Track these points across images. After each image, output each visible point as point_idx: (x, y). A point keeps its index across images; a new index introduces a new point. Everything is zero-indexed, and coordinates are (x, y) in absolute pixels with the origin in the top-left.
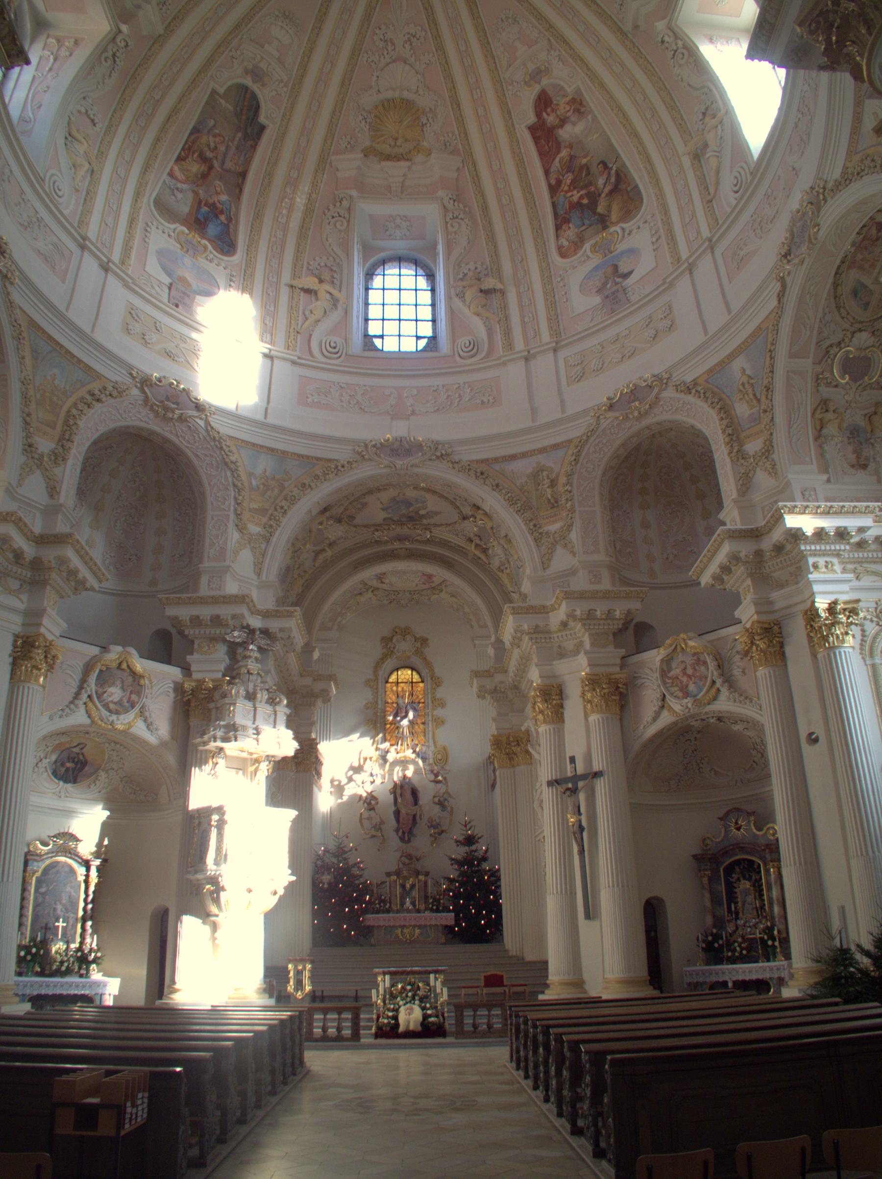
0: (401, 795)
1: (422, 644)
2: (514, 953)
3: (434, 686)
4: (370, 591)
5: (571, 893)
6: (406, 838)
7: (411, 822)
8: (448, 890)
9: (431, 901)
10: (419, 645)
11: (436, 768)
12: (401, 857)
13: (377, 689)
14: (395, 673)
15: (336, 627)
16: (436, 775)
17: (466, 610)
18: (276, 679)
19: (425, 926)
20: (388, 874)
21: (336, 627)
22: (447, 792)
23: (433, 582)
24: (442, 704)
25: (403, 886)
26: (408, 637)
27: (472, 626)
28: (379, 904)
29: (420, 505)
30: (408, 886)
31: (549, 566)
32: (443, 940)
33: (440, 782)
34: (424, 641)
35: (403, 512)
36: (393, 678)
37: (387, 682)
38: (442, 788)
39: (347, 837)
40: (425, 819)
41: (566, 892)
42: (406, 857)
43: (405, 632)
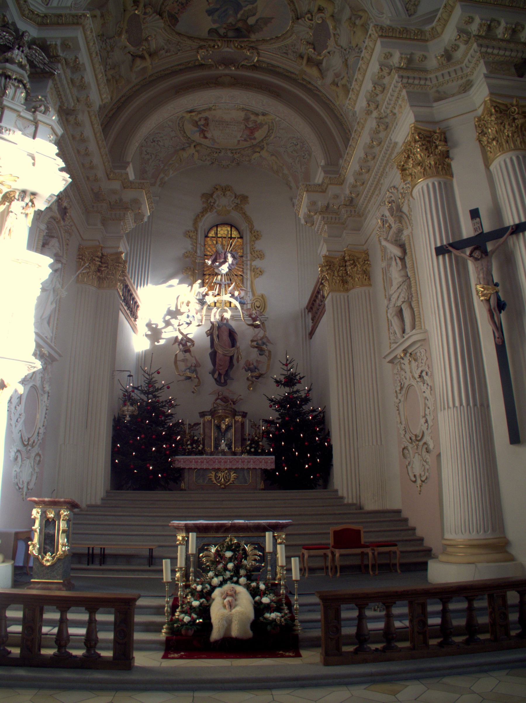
0: (218, 336)
1: (241, 201)
2: (350, 501)
3: (254, 238)
4: (192, 146)
5: (482, 405)
6: (223, 381)
7: (227, 363)
8: (267, 432)
9: (249, 442)
10: (238, 201)
11: (254, 312)
12: (216, 400)
13: (196, 239)
14: (215, 229)
15: (158, 183)
16: (254, 320)
17: (286, 171)
18: (60, 131)
19: (243, 469)
20: (203, 415)
21: (158, 183)
22: (265, 337)
23: (255, 139)
24: (261, 256)
25: (218, 427)
26: (228, 193)
27: (291, 188)
28: (191, 444)
29: (250, 7)
30: (223, 427)
31: (415, 12)
32: (262, 486)
33: (257, 326)
34: (244, 199)
35: (231, 20)
36: (212, 234)
37: (207, 236)
38: (260, 333)
39: (158, 373)
40: (242, 363)
41: (475, 405)
42: (221, 399)
43: (225, 189)
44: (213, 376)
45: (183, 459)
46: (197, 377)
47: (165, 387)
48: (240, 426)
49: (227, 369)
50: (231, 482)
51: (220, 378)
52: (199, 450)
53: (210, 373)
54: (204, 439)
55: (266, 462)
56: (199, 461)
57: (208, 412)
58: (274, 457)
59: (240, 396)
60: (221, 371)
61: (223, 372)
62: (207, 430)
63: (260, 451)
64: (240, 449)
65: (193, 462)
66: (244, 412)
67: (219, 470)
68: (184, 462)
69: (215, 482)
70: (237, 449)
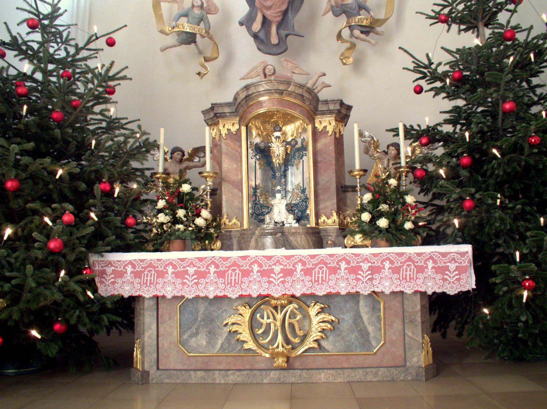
9: (368, 197)
19: (354, 296)
28: (171, 209)
44: (249, 29)
45: (130, 263)
46: (207, 32)
47: (101, 43)
48: (332, 148)
49: (284, 7)
50: (310, 343)
51: (268, 34)
52: (199, 229)
53: (241, 24)
54: (214, 192)
55: (441, 270)
56: (191, 270)
57: (228, 105)
58: (468, 248)
59: (324, 75)
60: (268, 13)
61: (274, 15)
62: (226, 164)
63: (408, 225)
64: (335, 217)
65: (170, 277)
66: (342, 103)
67: (264, 299)
68: (137, 274)
69: (251, 345)
70: (323, 218)
